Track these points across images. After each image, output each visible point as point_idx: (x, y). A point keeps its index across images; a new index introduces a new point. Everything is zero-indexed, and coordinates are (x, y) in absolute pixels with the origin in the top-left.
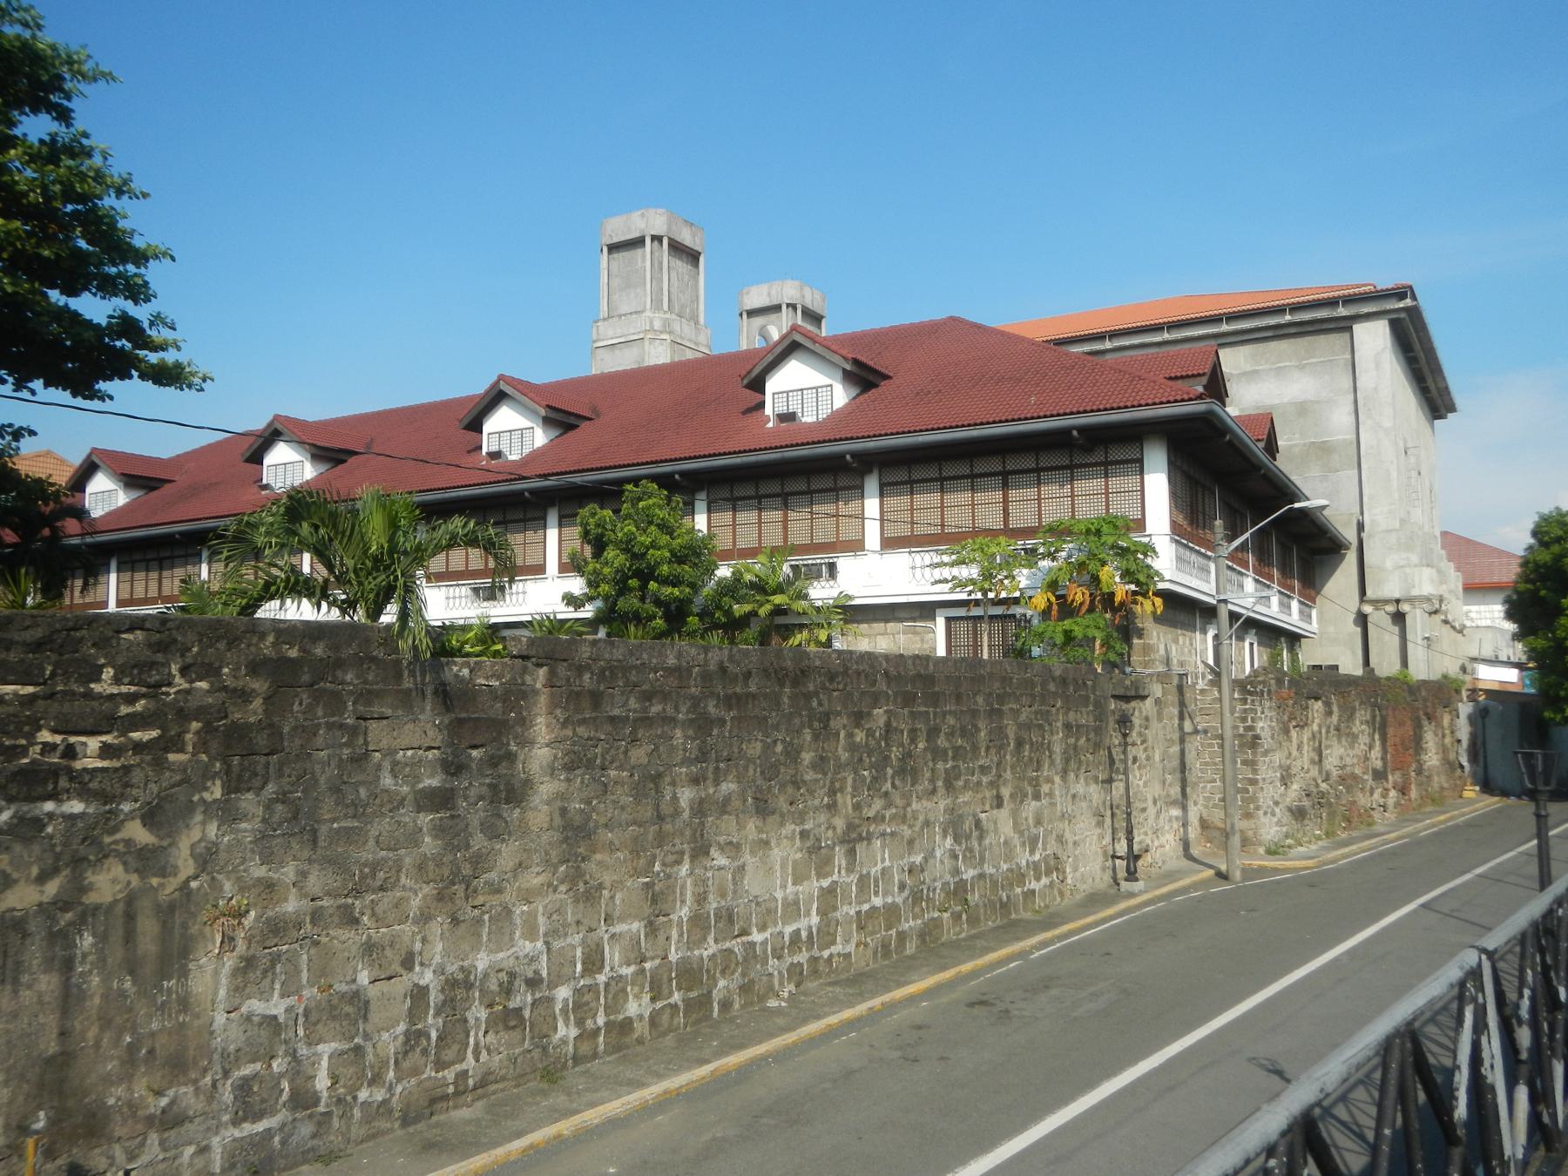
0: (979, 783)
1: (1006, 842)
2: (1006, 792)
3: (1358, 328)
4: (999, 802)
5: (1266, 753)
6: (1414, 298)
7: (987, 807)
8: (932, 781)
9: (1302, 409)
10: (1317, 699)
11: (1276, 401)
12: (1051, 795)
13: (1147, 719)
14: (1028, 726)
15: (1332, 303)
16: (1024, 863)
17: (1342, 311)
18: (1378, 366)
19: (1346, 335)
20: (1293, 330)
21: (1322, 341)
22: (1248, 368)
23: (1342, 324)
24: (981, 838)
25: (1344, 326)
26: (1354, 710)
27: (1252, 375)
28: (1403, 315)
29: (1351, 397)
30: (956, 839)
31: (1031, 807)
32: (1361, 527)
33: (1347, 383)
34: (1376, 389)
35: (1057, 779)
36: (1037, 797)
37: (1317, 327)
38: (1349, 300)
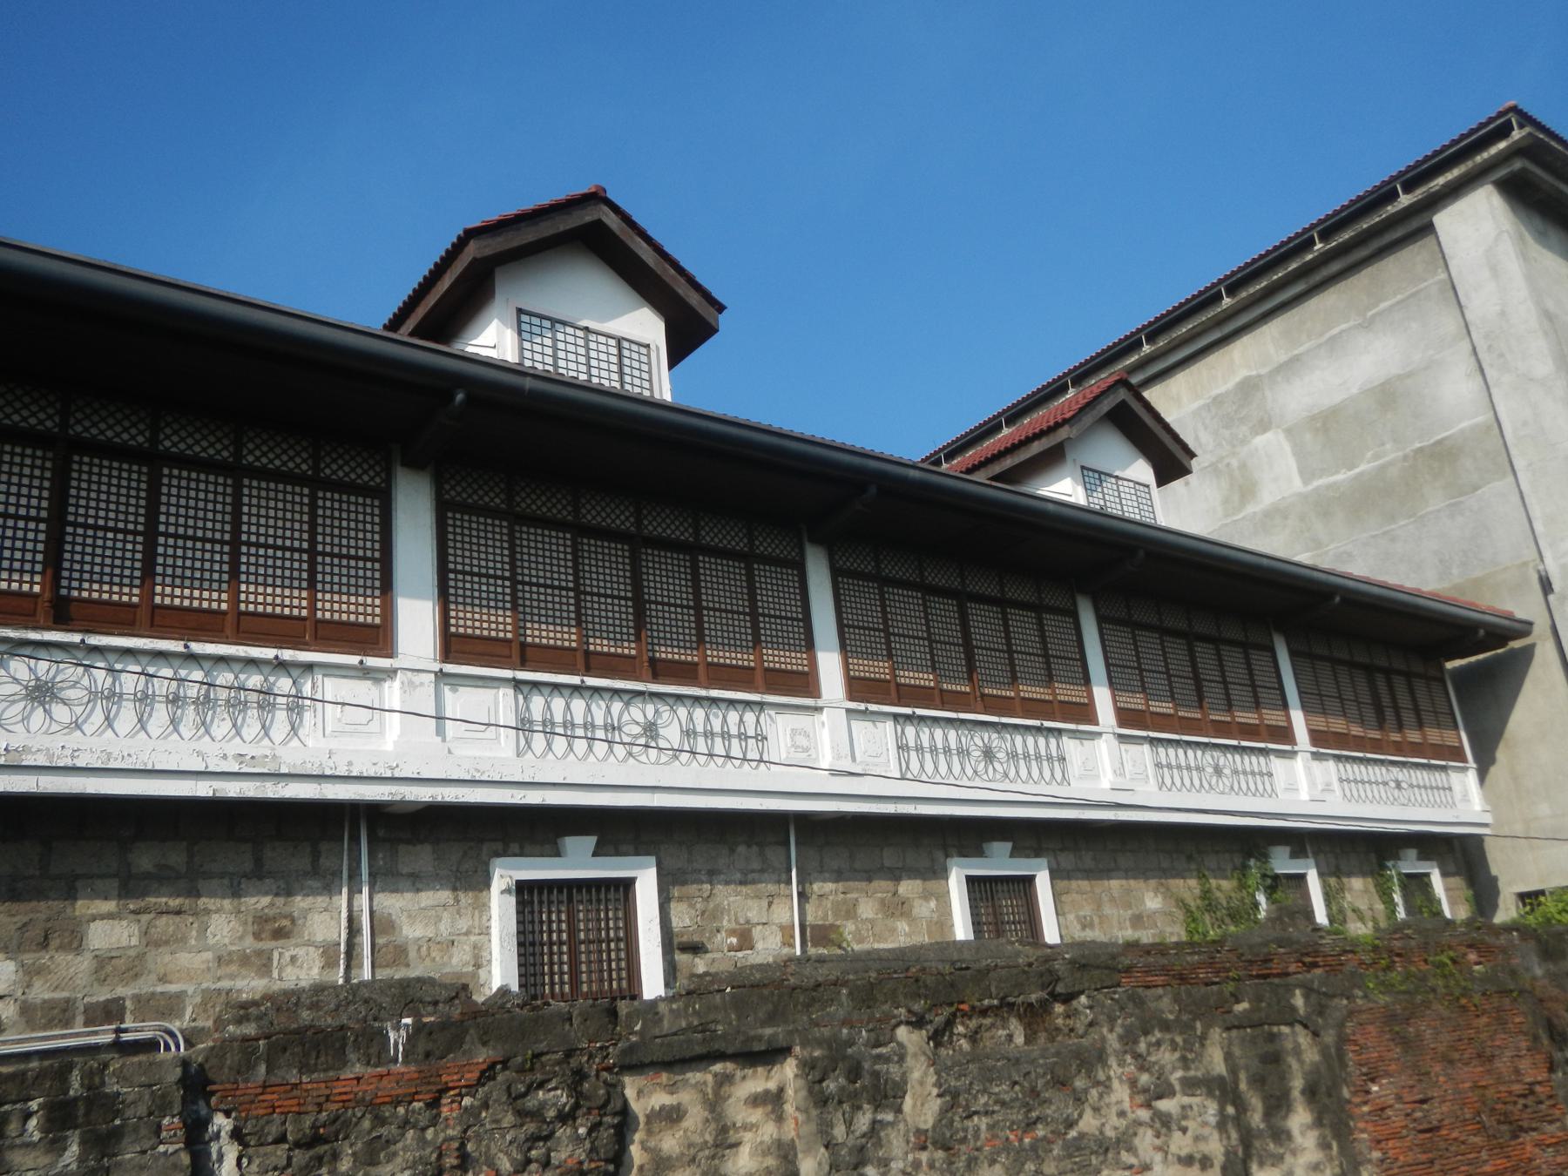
3: (1444, 220)
6: (1526, 119)
9: (1387, 395)
10: (771, 1055)
11: (1338, 398)
15: (1385, 194)
17: (1405, 200)
18: (1495, 271)
19: (1429, 241)
20: (1335, 267)
21: (1390, 267)
22: (1283, 358)
23: (1415, 224)
25: (1415, 227)
26: (1092, 1059)
27: (1290, 367)
28: (1518, 164)
29: (1465, 346)
32: (1546, 586)
33: (1450, 323)
34: (1503, 313)
37: (1375, 244)
38: (1413, 178)
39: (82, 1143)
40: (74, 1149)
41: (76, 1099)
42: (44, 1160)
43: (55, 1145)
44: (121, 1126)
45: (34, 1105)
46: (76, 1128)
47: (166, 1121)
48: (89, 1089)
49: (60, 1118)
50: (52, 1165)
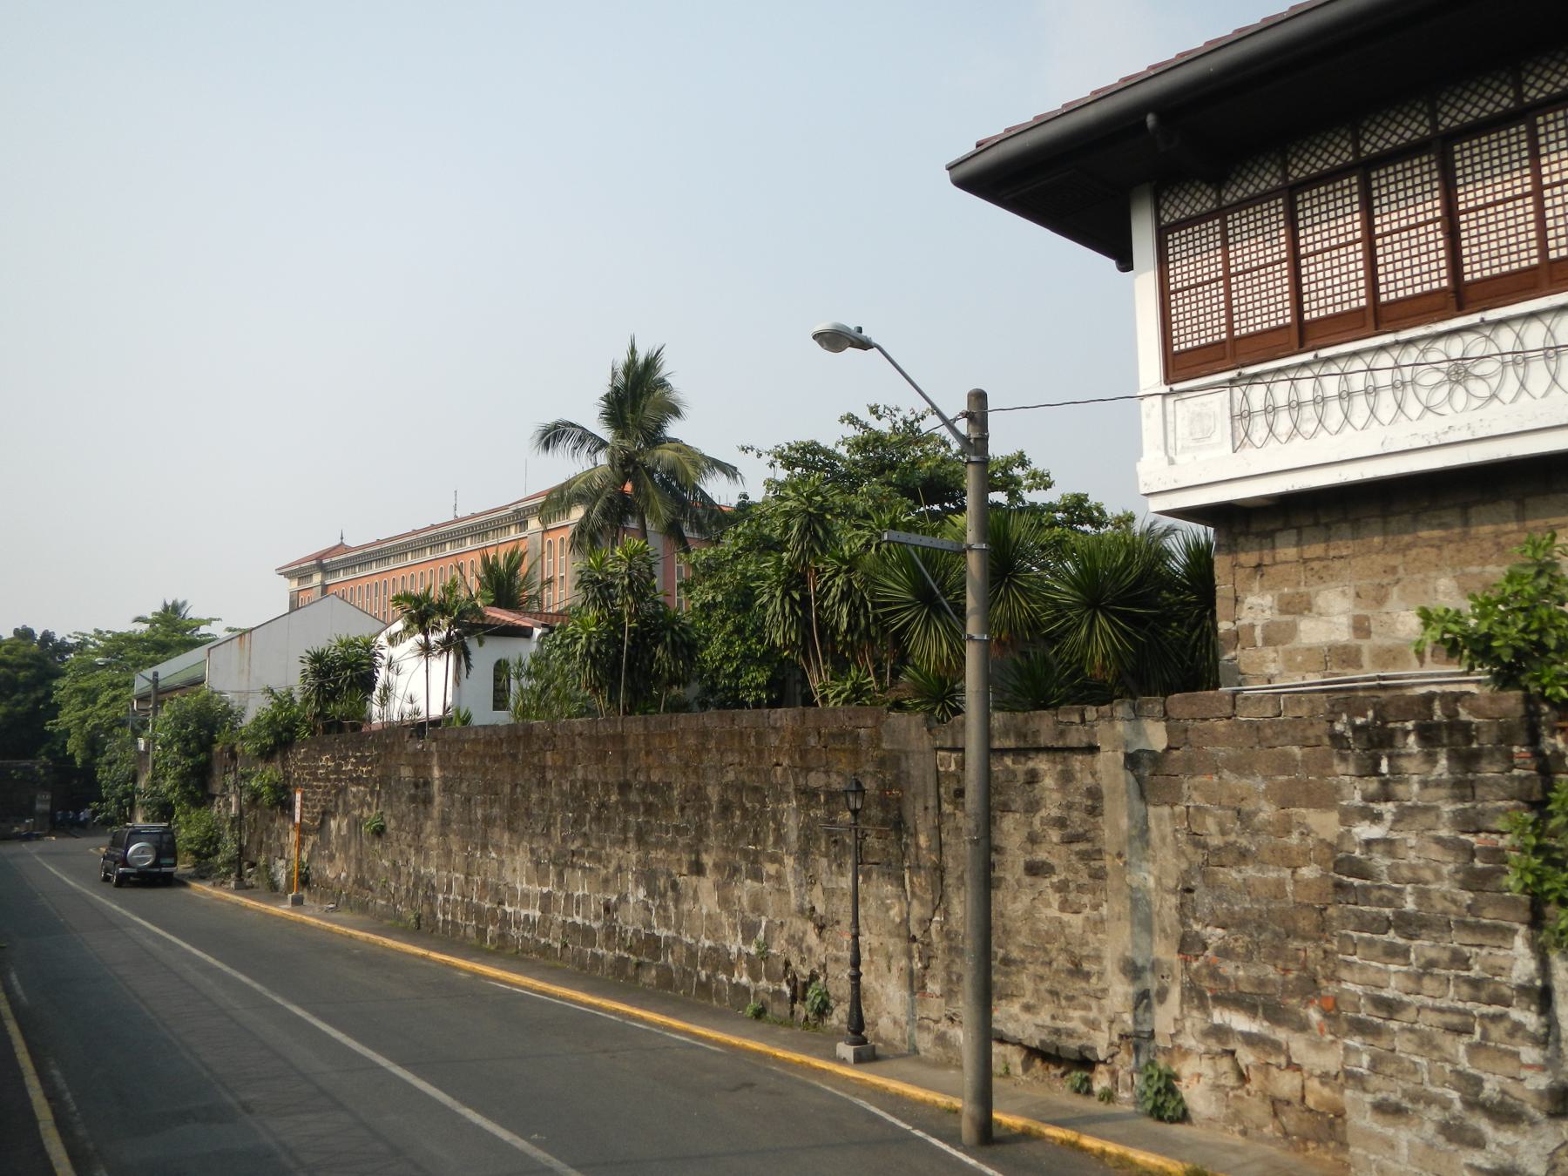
0: (674, 843)
1: (709, 916)
2: (708, 860)
4: (698, 869)
5: (1408, 925)
7: (684, 871)
8: (625, 830)
12: (779, 878)
13: (1095, 794)
14: (739, 788)
16: (734, 949)
24: (677, 901)
30: (650, 894)
31: (745, 889)
35: (789, 861)
36: (757, 875)
39: (1449, 759)
40: (1443, 762)
41: (1439, 725)
42: (1425, 768)
43: (1431, 759)
44: (1480, 750)
45: (1410, 725)
46: (1443, 746)
47: (1516, 749)
48: (1448, 717)
49: (1429, 735)
50: (1430, 772)
